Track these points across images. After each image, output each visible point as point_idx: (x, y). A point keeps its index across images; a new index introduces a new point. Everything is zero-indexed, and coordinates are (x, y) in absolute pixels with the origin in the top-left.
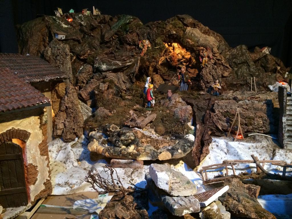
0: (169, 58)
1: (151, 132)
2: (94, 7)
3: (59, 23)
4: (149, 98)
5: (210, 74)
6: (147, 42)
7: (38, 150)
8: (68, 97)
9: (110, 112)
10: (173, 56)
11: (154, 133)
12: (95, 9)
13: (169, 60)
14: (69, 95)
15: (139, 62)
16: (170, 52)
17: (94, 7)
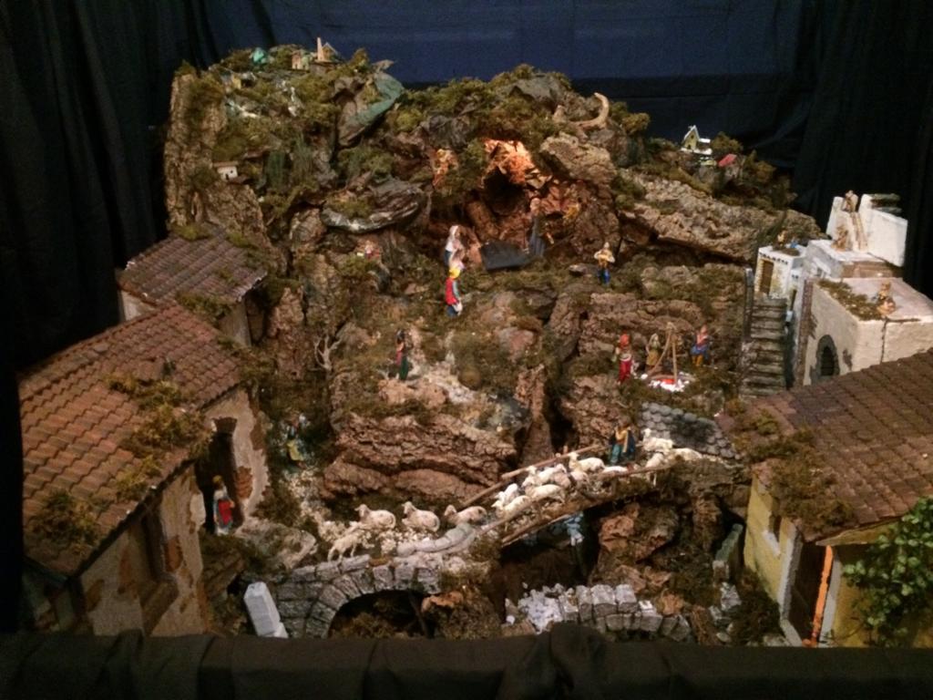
0: (504, 167)
1: (450, 383)
2: (319, 40)
3: (236, 109)
4: (450, 300)
5: (593, 223)
6: (446, 155)
7: (250, 443)
8: (281, 310)
9: (370, 334)
10: (514, 163)
11: (456, 383)
12: (323, 44)
13: (504, 171)
14: (284, 307)
15: (430, 203)
16: (507, 152)
17: (319, 40)
